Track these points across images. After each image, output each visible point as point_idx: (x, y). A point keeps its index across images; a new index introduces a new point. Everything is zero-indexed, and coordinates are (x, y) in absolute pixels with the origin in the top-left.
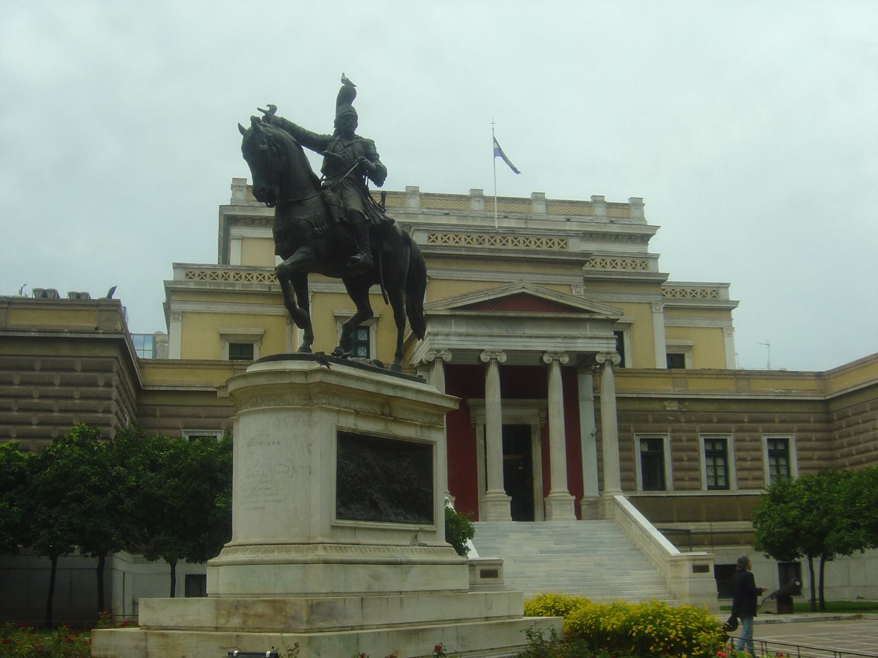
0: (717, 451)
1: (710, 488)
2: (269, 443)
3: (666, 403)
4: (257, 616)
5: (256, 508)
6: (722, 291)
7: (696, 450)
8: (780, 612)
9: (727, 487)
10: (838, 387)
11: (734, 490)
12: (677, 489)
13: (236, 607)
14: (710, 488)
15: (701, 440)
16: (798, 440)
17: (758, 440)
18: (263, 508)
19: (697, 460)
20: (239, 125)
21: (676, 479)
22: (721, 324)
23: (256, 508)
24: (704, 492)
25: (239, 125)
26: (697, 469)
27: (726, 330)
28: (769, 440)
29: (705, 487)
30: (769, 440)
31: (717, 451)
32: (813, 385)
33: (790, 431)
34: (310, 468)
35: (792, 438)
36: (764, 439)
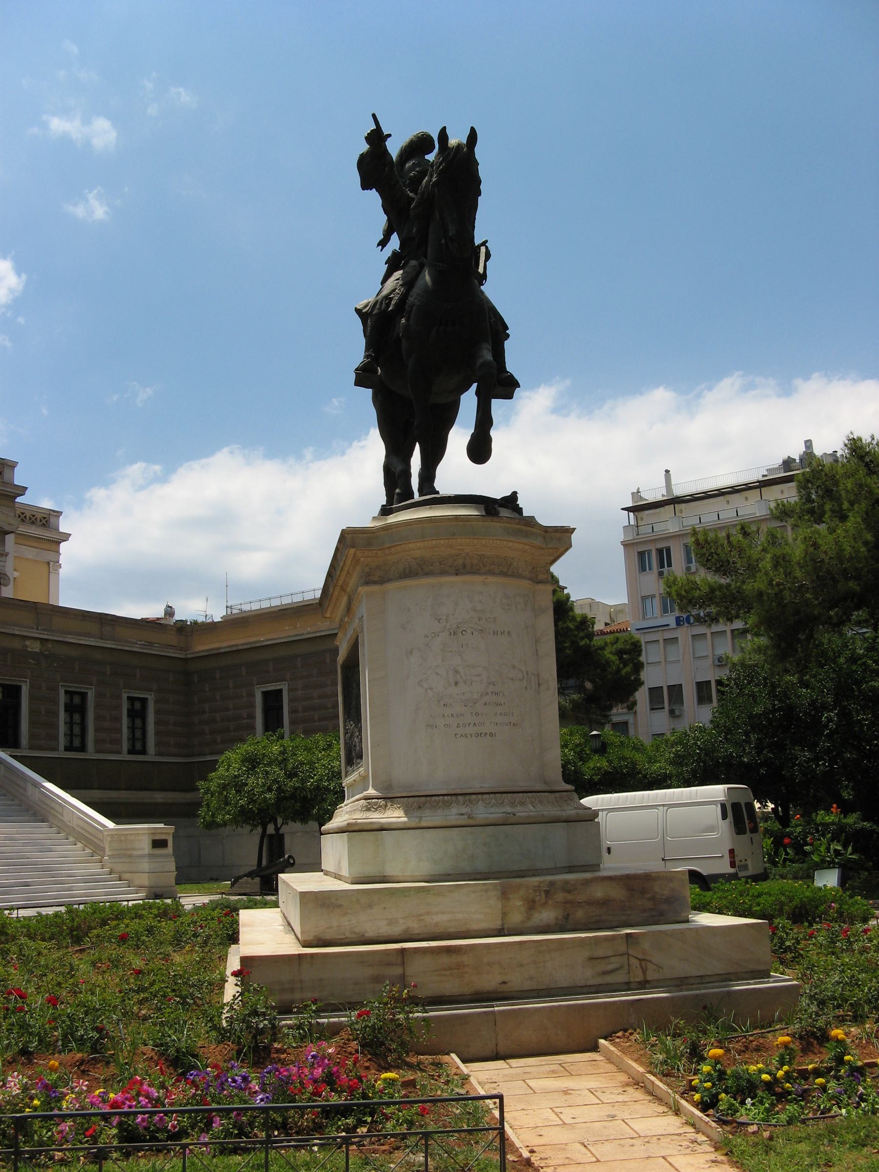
0: (76, 707)
1: (67, 749)
2: (495, 633)
3: (28, 643)
4: (590, 903)
5: (479, 735)
6: (52, 520)
7: (57, 703)
8: (262, 894)
9: (82, 748)
10: (202, 646)
11: (91, 754)
12: (32, 747)
13: (547, 892)
14: (67, 749)
15: (62, 692)
16: (157, 701)
17: (119, 697)
18: (491, 735)
19: (56, 714)
20: (444, 129)
21: (32, 736)
22: (49, 556)
23: (479, 735)
24: (61, 754)
25: (444, 129)
26: (55, 726)
27: (52, 565)
28: (129, 698)
29: (62, 747)
30: (129, 698)
31: (76, 707)
32: (172, 638)
33: (150, 690)
34: (538, 676)
35: (151, 697)
36: (125, 696)
